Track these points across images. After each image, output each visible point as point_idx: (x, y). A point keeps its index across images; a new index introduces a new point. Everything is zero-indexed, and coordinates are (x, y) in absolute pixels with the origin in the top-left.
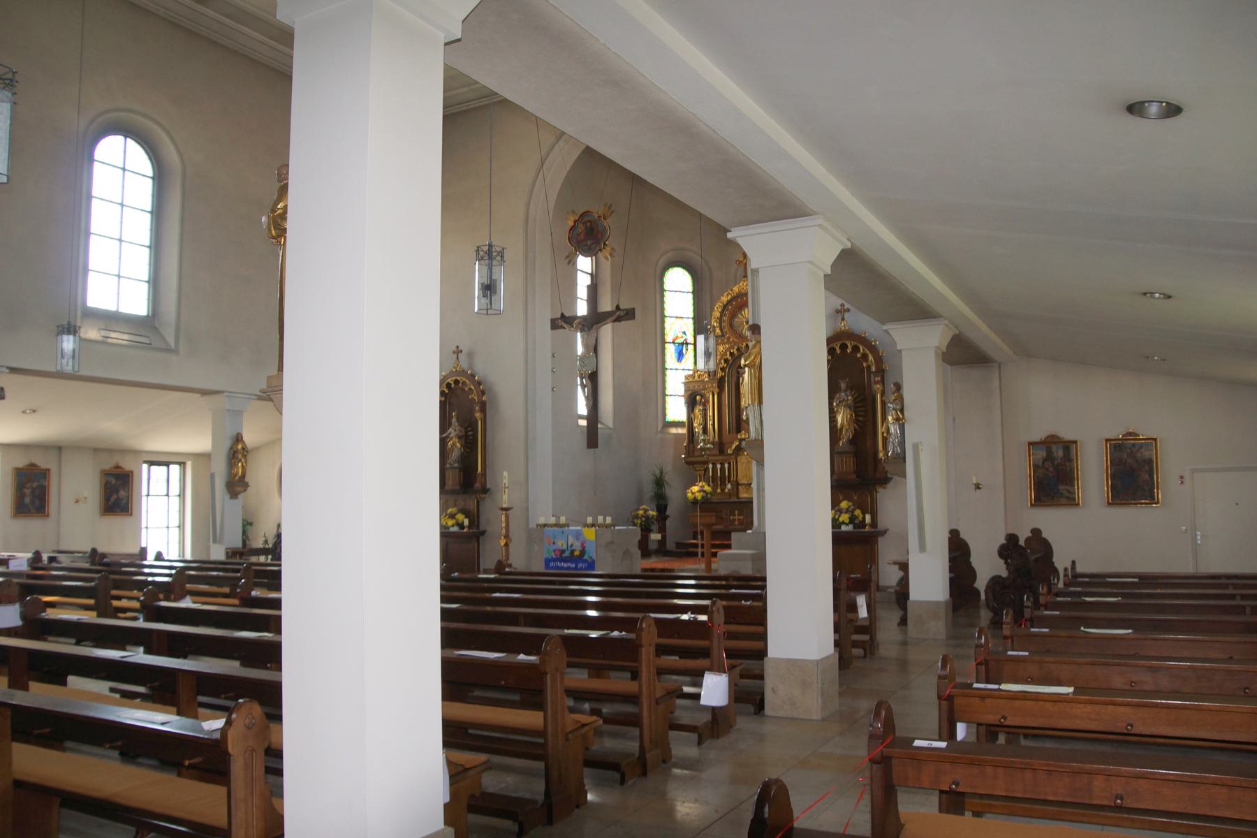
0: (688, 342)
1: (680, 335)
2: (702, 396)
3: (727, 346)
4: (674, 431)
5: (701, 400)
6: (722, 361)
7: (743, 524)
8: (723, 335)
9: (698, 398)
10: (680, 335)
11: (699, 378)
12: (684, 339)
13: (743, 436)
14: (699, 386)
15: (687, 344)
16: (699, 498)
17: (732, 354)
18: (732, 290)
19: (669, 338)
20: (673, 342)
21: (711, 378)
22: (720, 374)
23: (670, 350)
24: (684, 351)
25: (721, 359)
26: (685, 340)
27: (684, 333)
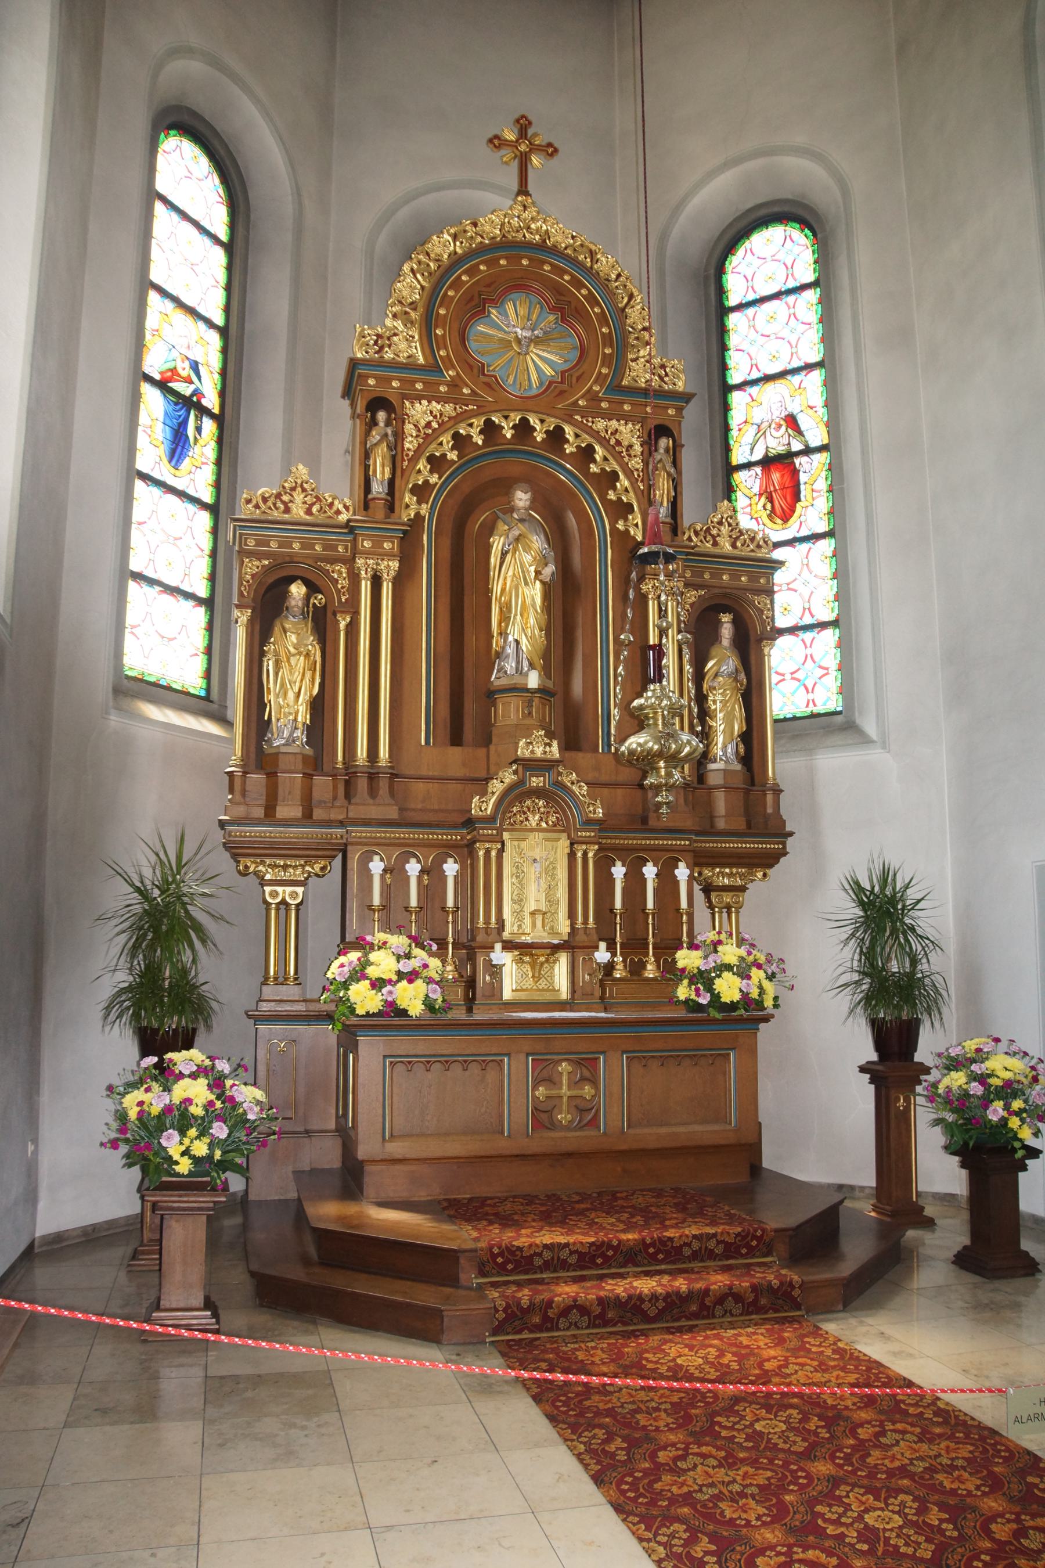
0: (205, 402)
1: (185, 370)
2: (312, 588)
3: (449, 409)
4: (153, 712)
5: (307, 598)
6: (422, 465)
7: (594, 1122)
8: (433, 368)
9: (297, 590)
10: (185, 370)
11: (309, 512)
12: (192, 388)
13: (539, 751)
14: (307, 545)
15: (203, 411)
16: (416, 1009)
17: (460, 442)
18: (475, 225)
19: (154, 363)
20: (162, 385)
21: (379, 511)
22: (410, 506)
23: (153, 401)
24: (191, 431)
25: (419, 451)
26: (196, 392)
27: (195, 366)
